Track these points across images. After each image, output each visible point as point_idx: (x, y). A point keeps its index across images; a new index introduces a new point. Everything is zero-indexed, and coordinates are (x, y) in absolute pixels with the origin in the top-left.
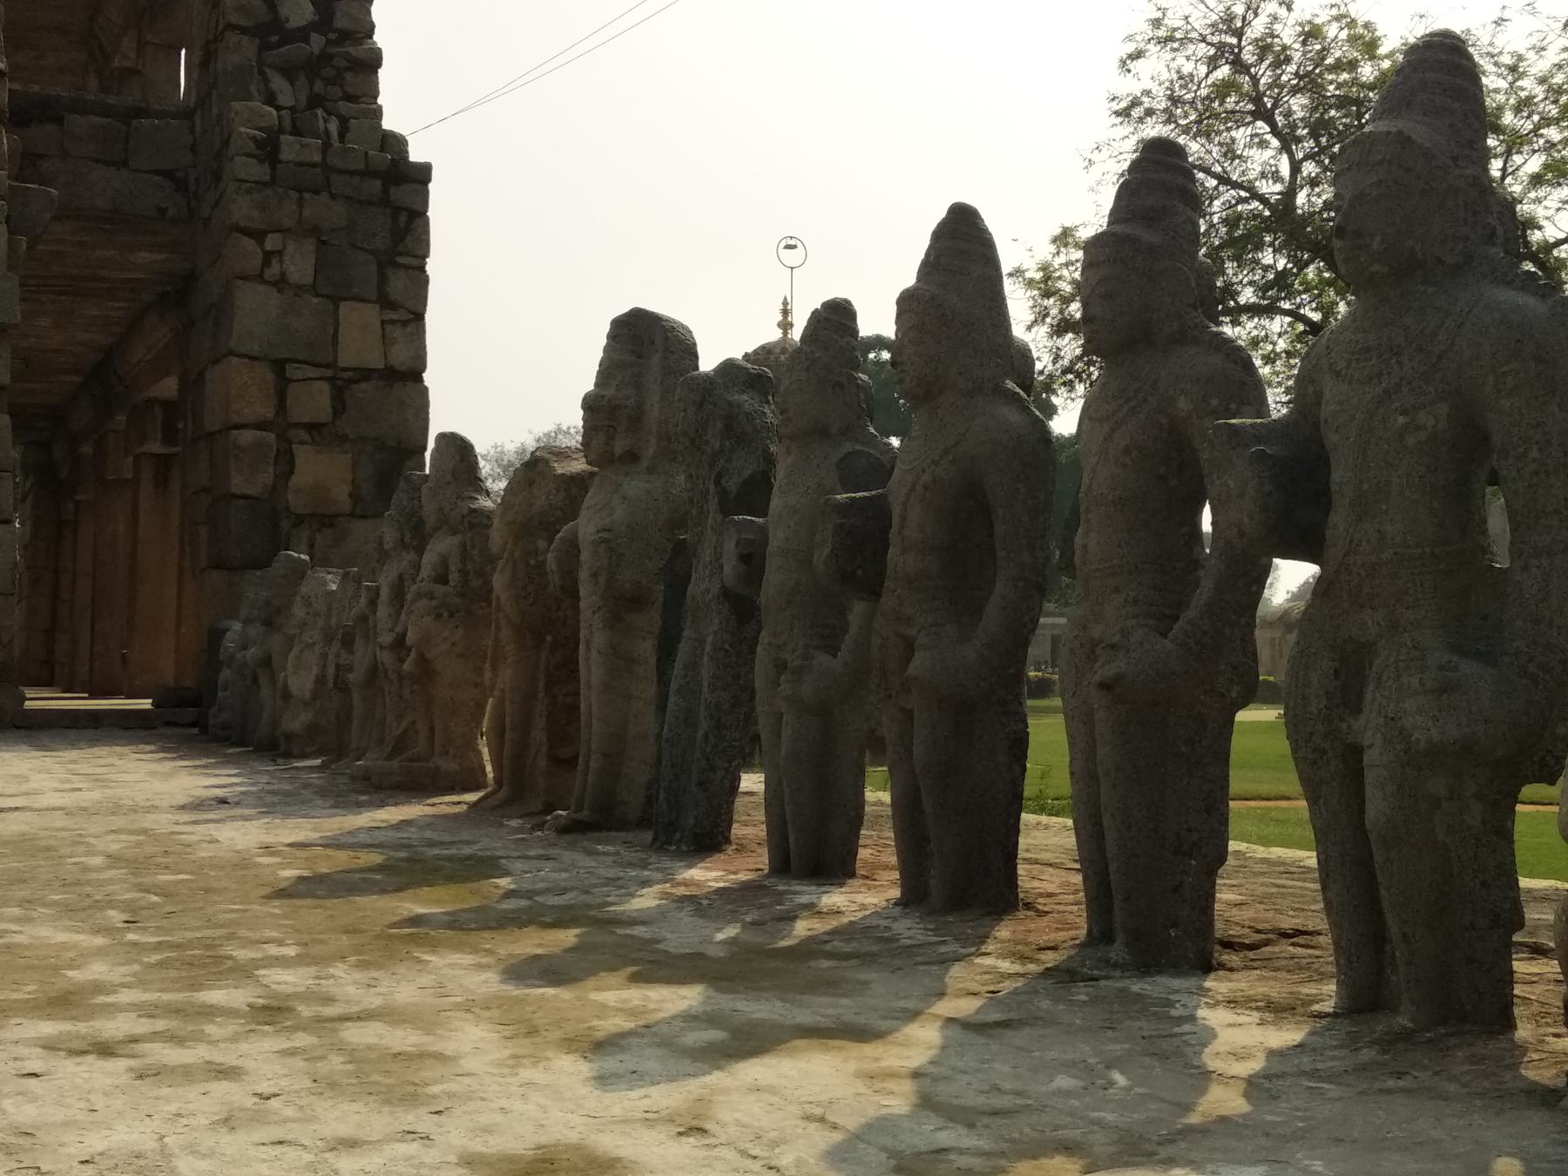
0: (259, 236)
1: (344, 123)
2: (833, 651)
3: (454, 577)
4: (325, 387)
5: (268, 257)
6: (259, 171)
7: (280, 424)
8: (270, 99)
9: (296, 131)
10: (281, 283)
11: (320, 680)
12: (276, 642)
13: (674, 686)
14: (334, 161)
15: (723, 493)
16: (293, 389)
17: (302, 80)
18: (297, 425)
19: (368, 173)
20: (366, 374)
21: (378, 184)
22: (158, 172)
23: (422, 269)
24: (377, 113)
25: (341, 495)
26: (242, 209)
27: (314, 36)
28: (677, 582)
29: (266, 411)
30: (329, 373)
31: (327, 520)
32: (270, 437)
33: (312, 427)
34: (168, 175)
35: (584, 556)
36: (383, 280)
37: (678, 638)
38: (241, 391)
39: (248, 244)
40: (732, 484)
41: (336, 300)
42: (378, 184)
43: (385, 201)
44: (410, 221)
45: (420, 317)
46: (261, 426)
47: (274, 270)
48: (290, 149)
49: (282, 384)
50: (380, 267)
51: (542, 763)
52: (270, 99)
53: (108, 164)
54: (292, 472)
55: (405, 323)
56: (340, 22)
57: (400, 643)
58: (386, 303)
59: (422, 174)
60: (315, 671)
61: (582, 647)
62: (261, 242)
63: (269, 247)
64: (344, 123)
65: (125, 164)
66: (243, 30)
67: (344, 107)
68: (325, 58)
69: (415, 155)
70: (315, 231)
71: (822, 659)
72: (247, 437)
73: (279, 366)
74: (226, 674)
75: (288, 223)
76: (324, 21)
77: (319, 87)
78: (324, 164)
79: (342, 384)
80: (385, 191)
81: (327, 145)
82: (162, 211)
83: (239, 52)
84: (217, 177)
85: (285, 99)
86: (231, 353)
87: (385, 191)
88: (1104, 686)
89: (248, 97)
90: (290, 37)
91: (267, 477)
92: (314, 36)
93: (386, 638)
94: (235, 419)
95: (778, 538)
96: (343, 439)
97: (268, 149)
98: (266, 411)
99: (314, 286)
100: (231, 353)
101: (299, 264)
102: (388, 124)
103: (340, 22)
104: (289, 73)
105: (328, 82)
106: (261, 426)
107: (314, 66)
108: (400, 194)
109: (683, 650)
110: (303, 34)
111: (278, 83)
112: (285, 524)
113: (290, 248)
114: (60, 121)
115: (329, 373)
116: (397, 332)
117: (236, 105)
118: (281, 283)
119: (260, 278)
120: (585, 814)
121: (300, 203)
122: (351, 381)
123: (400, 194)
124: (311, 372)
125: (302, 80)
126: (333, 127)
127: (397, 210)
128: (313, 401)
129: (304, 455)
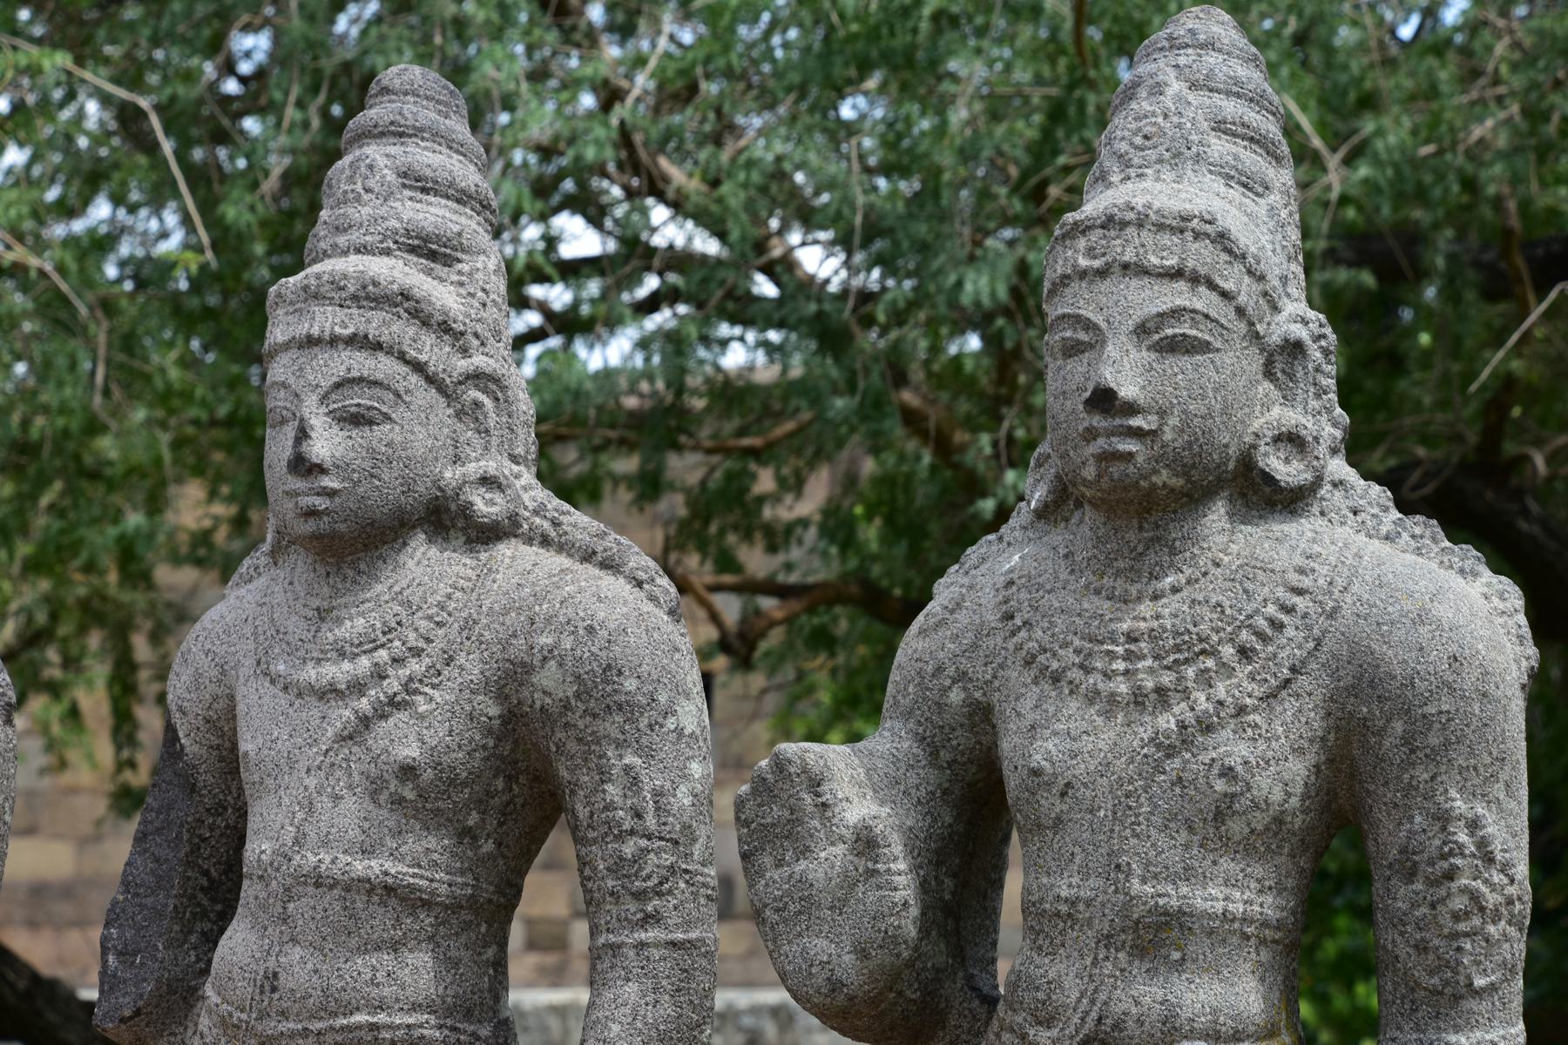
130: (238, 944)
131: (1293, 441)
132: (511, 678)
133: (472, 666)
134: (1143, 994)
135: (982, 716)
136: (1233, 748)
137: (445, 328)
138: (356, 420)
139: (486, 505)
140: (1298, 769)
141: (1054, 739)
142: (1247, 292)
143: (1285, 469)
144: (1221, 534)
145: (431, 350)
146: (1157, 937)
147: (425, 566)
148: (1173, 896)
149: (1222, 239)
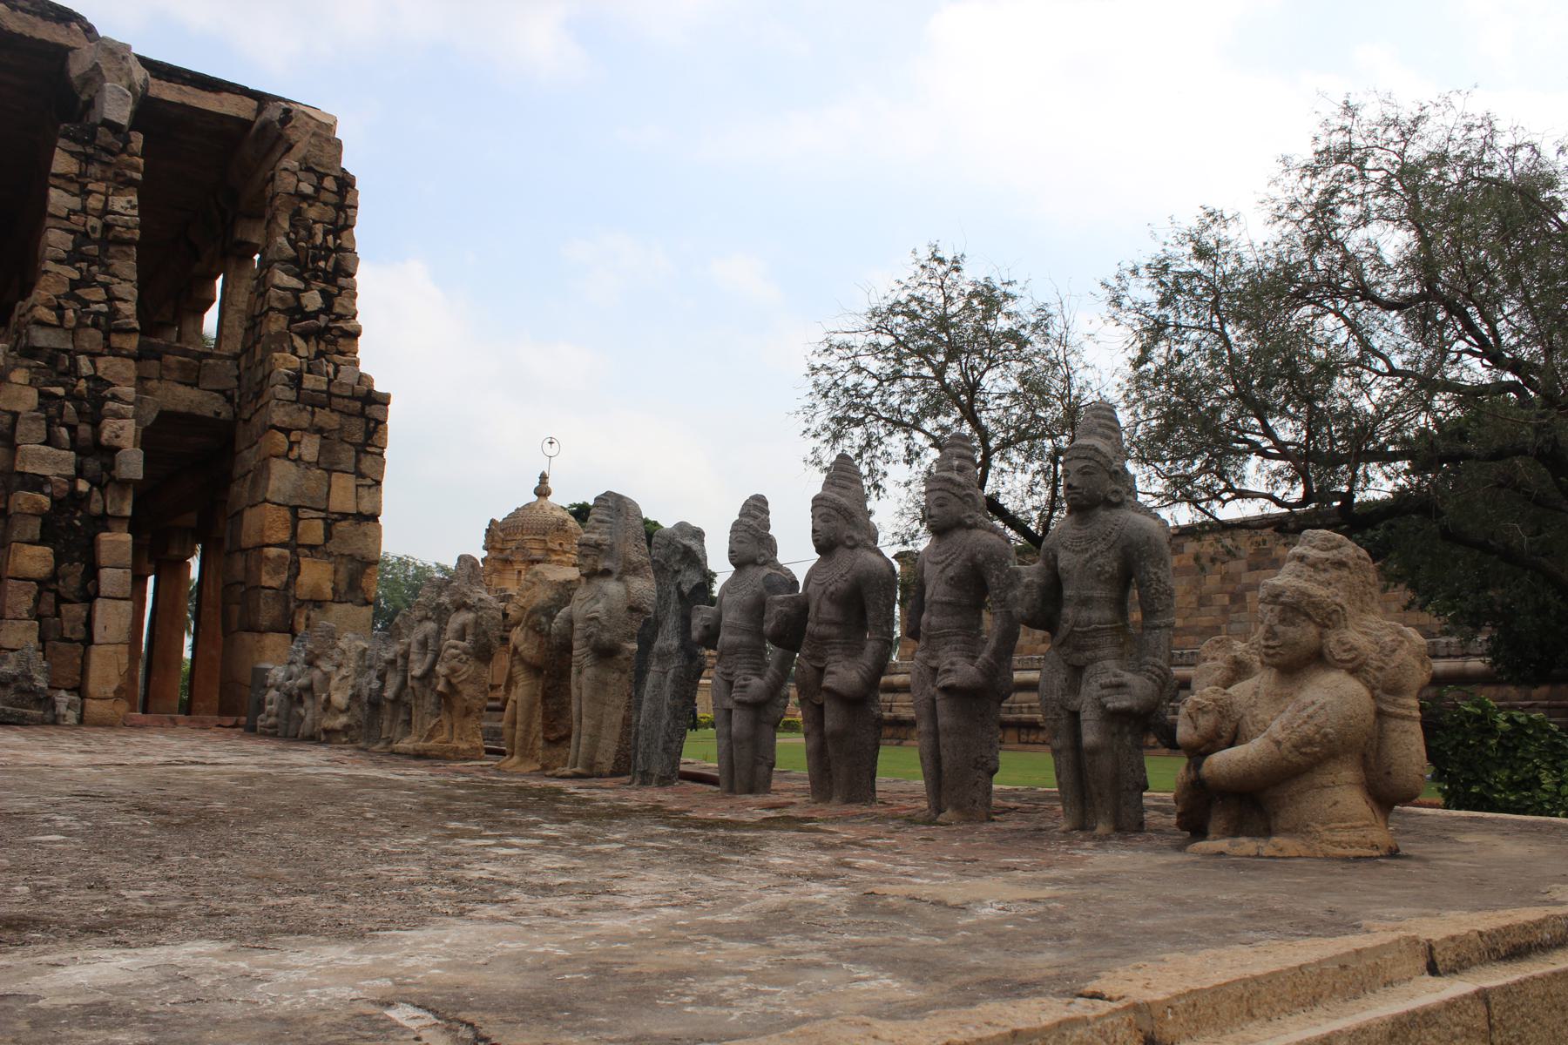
0: (287, 431)
1: (337, 367)
2: (761, 676)
3: (469, 637)
4: (320, 522)
5: (292, 444)
6: (291, 394)
7: (293, 545)
8: (294, 352)
9: (310, 371)
10: (298, 460)
11: (355, 697)
12: (317, 674)
13: (646, 696)
14: (335, 390)
15: (681, 594)
16: (301, 524)
17: (313, 341)
18: (304, 546)
19: (353, 398)
20: (345, 516)
21: (359, 404)
22: (217, 391)
23: (381, 455)
24: (356, 363)
25: (327, 591)
26: (279, 416)
27: (322, 317)
28: (646, 642)
29: (284, 536)
30: (323, 515)
31: (318, 603)
32: (287, 552)
33: (312, 547)
34: (223, 392)
35: (578, 625)
36: (358, 461)
37: (647, 672)
38: (266, 524)
39: (281, 436)
40: (686, 589)
41: (330, 471)
42: (359, 404)
43: (362, 414)
44: (375, 428)
45: (379, 483)
46: (281, 545)
47: (294, 454)
48: (309, 382)
49: (296, 519)
50: (358, 453)
51: (540, 743)
52: (294, 352)
53: (186, 385)
54: (298, 573)
55: (370, 487)
56: (338, 309)
57: (429, 674)
58: (360, 474)
59: (384, 400)
60: (350, 692)
61: (573, 677)
62: (288, 437)
63: (293, 438)
64: (337, 367)
65: (196, 385)
66: (280, 311)
67: (337, 358)
68: (328, 329)
69: (379, 387)
70: (320, 430)
71: (755, 681)
72: (273, 552)
73: (294, 510)
74: (273, 693)
75: (305, 425)
76: (328, 308)
77: (322, 346)
78: (330, 395)
79: (331, 521)
80: (363, 408)
81: (330, 381)
82: (218, 414)
83: (277, 324)
84: (259, 395)
85: (303, 352)
86: (266, 501)
87: (363, 408)
88: (945, 689)
89: (283, 350)
90: (307, 316)
91: (284, 577)
92: (322, 317)
93: (417, 671)
94: (267, 541)
95: (729, 617)
96: (330, 555)
97: (296, 380)
98: (284, 536)
99: (317, 463)
100: (266, 501)
101: (310, 448)
102: (363, 369)
103: (338, 309)
104: (305, 336)
105: (328, 342)
106: (281, 545)
107: (319, 334)
108: (373, 411)
109: (651, 679)
110: (315, 315)
111: (299, 342)
112: (292, 605)
113: (305, 440)
114: (159, 359)
115: (323, 515)
116: (364, 492)
117: (276, 355)
118: (298, 460)
119: (286, 456)
120: (578, 769)
121: (313, 413)
122: (336, 520)
123: (373, 411)
124: (314, 514)
125: (313, 341)
126: (331, 369)
127: (368, 419)
128: (313, 532)
129: (305, 564)
130: (925, 616)
131: (1116, 492)
132: (972, 558)
133: (965, 555)
134: (1084, 614)
135: (1055, 557)
136: (1100, 560)
137: (959, 485)
138: (941, 506)
139: (969, 521)
140: (1115, 564)
141: (1065, 560)
142: (1103, 460)
143: (1114, 499)
144: (1103, 514)
145: (955, 490)
146: (1085, 602)
147: (959, 536)
148: (1089, 593)
149: (1096, 450)
